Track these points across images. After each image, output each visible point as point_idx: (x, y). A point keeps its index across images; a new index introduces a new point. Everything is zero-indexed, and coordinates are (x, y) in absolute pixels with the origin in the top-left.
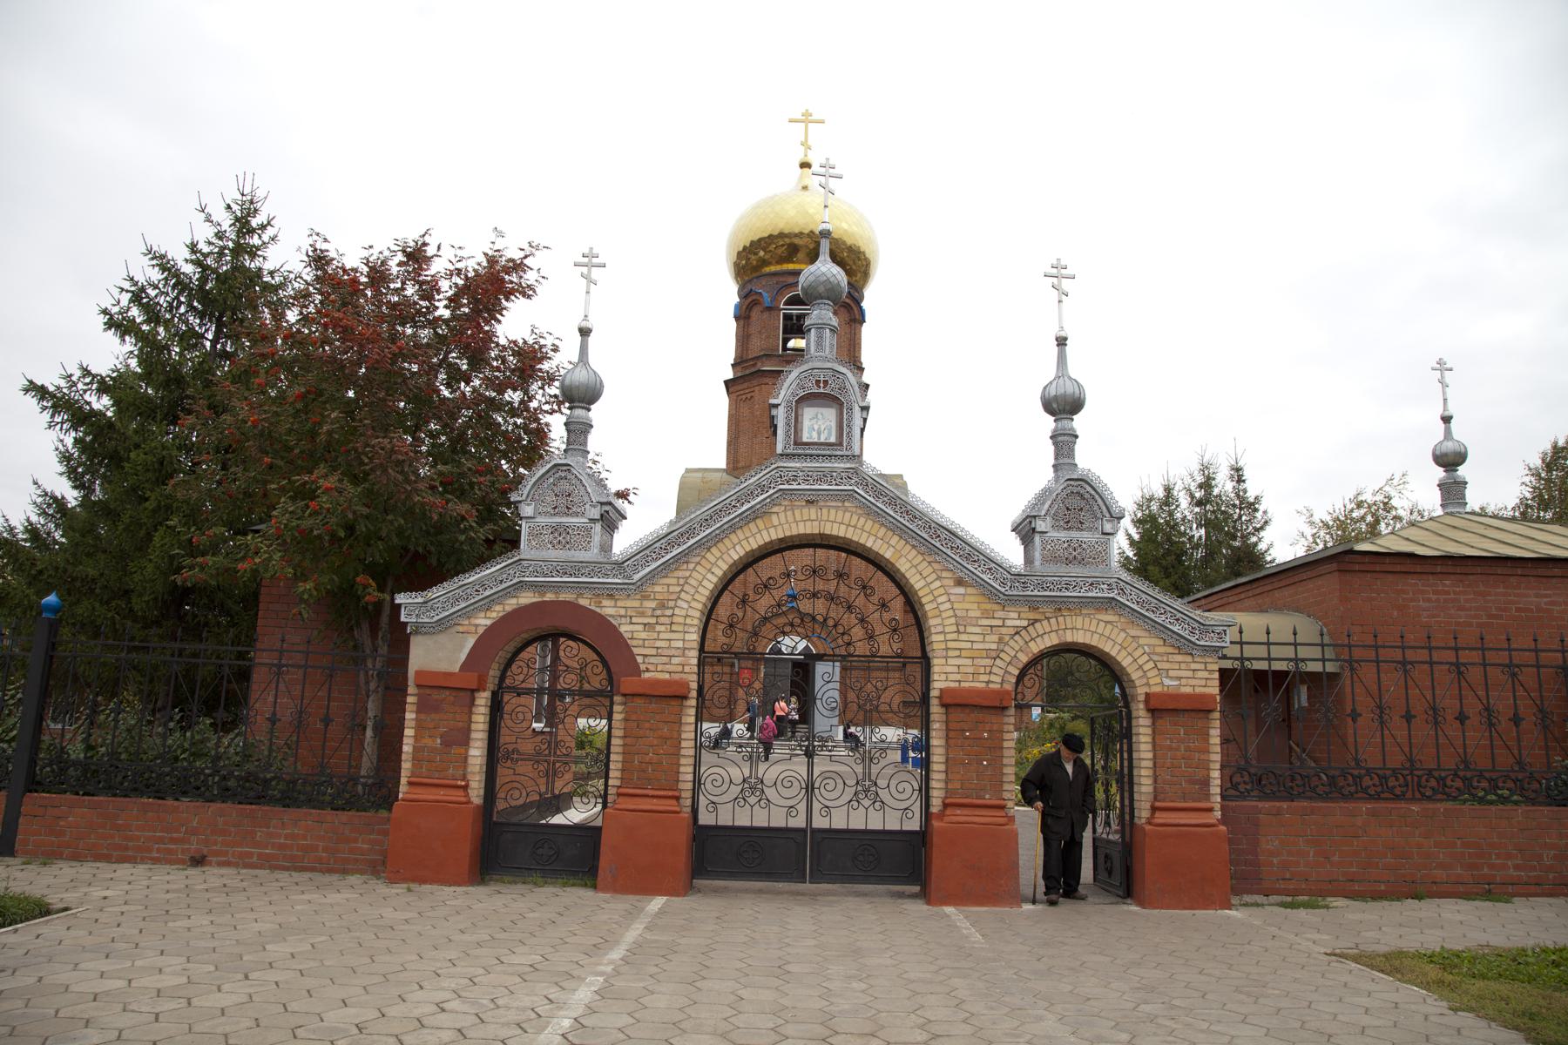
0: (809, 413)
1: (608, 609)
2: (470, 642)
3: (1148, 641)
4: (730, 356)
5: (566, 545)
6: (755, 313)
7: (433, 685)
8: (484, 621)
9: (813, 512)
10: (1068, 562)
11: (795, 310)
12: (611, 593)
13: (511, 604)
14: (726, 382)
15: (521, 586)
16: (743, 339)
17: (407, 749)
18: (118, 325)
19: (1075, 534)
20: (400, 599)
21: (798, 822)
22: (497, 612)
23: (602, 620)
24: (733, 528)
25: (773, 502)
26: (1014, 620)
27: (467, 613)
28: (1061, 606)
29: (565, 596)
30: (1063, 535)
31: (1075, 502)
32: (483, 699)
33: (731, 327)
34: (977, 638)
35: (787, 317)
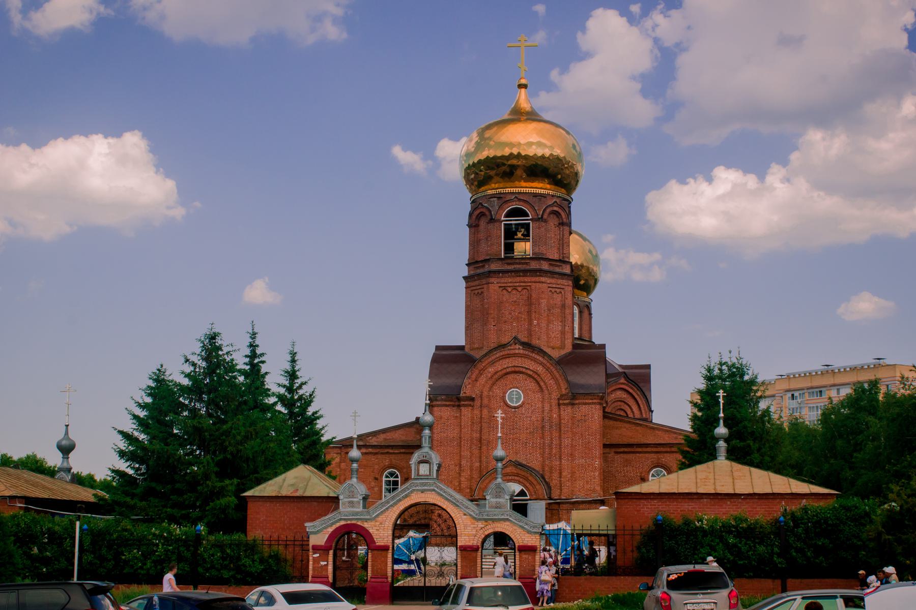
0: (421, 465)
1: (366, 525)
2: (327, 536)
3: (519, 530)
4: (465, 258)
5: (353, 507)
6: (483, 223)
7: (316, 548)
8: (330, 530)
9: (423, 495)
10: (496, 508)
11: (514, 221)
12: (366, 520)
13: (338, 525)
14: (465, 278)
15: (341, 519)
16: (474, 244)
17: (311, 567)
18: (149, 395)
19: (498, 500)
20: (306, 524)
21: (422, 584)
22: (334, 527)
24: (400, 500)
25: (412, 492)
27: (325, 528)
28: (494, 520)
29: (353, 522)
30: (495, 500)
31: (498, 490)
32: (331, 552)
33: (465, 233)
34: (470, 531)
35: (508, 228)
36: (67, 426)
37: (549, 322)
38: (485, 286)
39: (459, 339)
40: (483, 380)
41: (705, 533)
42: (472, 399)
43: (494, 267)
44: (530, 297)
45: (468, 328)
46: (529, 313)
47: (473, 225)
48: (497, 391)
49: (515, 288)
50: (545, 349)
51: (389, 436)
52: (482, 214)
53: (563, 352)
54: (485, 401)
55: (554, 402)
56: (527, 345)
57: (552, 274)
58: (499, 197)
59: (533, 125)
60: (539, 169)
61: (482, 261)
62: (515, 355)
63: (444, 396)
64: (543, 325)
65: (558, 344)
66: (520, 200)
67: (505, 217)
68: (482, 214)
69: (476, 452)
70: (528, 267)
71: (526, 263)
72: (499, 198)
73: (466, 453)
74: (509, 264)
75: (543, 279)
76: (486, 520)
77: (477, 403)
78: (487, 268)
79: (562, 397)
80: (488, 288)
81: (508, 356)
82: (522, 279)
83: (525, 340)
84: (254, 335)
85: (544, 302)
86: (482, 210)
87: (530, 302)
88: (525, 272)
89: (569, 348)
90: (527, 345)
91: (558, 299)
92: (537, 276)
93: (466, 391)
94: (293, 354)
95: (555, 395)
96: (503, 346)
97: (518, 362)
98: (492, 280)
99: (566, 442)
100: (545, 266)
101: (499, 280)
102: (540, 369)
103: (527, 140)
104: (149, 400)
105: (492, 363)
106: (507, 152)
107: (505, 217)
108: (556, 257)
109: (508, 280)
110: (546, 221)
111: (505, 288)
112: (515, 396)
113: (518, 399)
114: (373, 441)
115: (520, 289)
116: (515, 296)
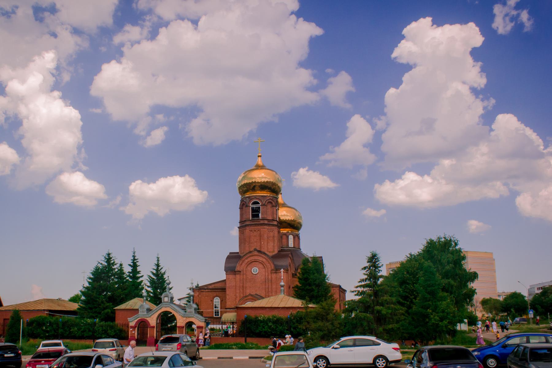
1: (147, 319)
7: (132, 327)
8: (136, 321)
11: (255, 206)
26: (185, 319)
28: (189, 317)
33: (238, 211)
37: (268, 243)
39: (236, 249)
40: (244, 264)
41: (261, 322)
42: (240, 272)
43: (247, 223)
45: (240, 246)
46: (260, 239)
47: (241, 208)
48: (249, 268)
49: (255, 231)
50: (266, 253)
51: (216, 285)
53: (274, 254)
54: (245, 272)
55: (269, 272)
56: (259, 251)
57: (269, 225)
58: (249, 197)
59: (264, 170)
60: (264, 186)
62: (255, 255)
63: (230, 269)
64: (266, 244)
65: (272, 250)
69: (242, 291)
73: (238, 291)
77: (242, 273)
79: (272, 270)
81: (253, 256)
83: (259, 249)
84: (134, 253)
85: (265, 236)
87: (260, 236)
88: (258, 225)
89: (276, 252)
90: (259, 251)
91: (272, 234)
93: (238, 269)
94: (158, 258)
95: (270, 270)
96: (251, 252)
97: (256, 258)
99: (274, 286)
100: (266, 222)
102: (264, 260)
103: (260, 176)
104: (92, 277)
105: (247, 258)
106: (254, 181)
108: (271, 218)
109: (252, 228)
110: (266, 206)
111: (251, 231)
112: (255, 270)
113: (256, 271)
114: (210, 287)
116: (255, 233)
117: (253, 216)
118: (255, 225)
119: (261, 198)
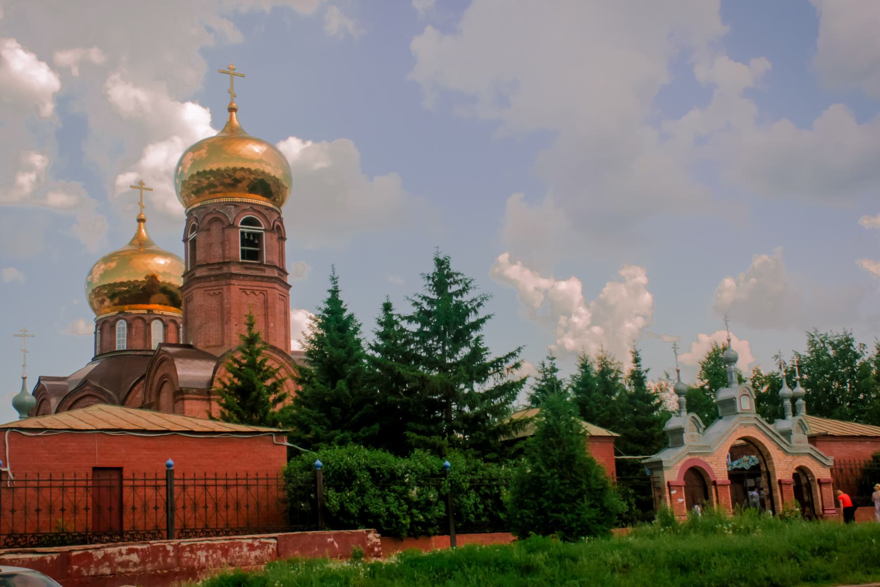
1: (707, 460)
2: (677, 472)
8: (679, 465)
11: (248, 229)
23: (705, 463)
26: (789, 459)
28: (798, 454)
29: (697, 456)
35: (243, 233)
36: (24, 378)
38: (225, 288)
43: (234, 270)
44: (266, 302)
52: (216, 220)
58: (236, 205)
61: (219, 263)
66: (255, 210)
67: (242, 224)
68: (216, 220)
70: (263, 274)
71: (261, 270)
72: (236, 206)
74: (246, 268)
75: (277, 286)
76: (793, 454)
78: (225, 270)
80: (229, 290)
82: (259, 284)
86: (216, 215)
88: (262, 279)
92: (272, 282)
98: (233, 282)
101: (239, 282)
107: (242, 224)
109: (248, 283)
111: (244, 291)
115: (257, 293)
116: (252, 300)
117: (246, 255)
118: (255, 277)
119: (265, 212)
